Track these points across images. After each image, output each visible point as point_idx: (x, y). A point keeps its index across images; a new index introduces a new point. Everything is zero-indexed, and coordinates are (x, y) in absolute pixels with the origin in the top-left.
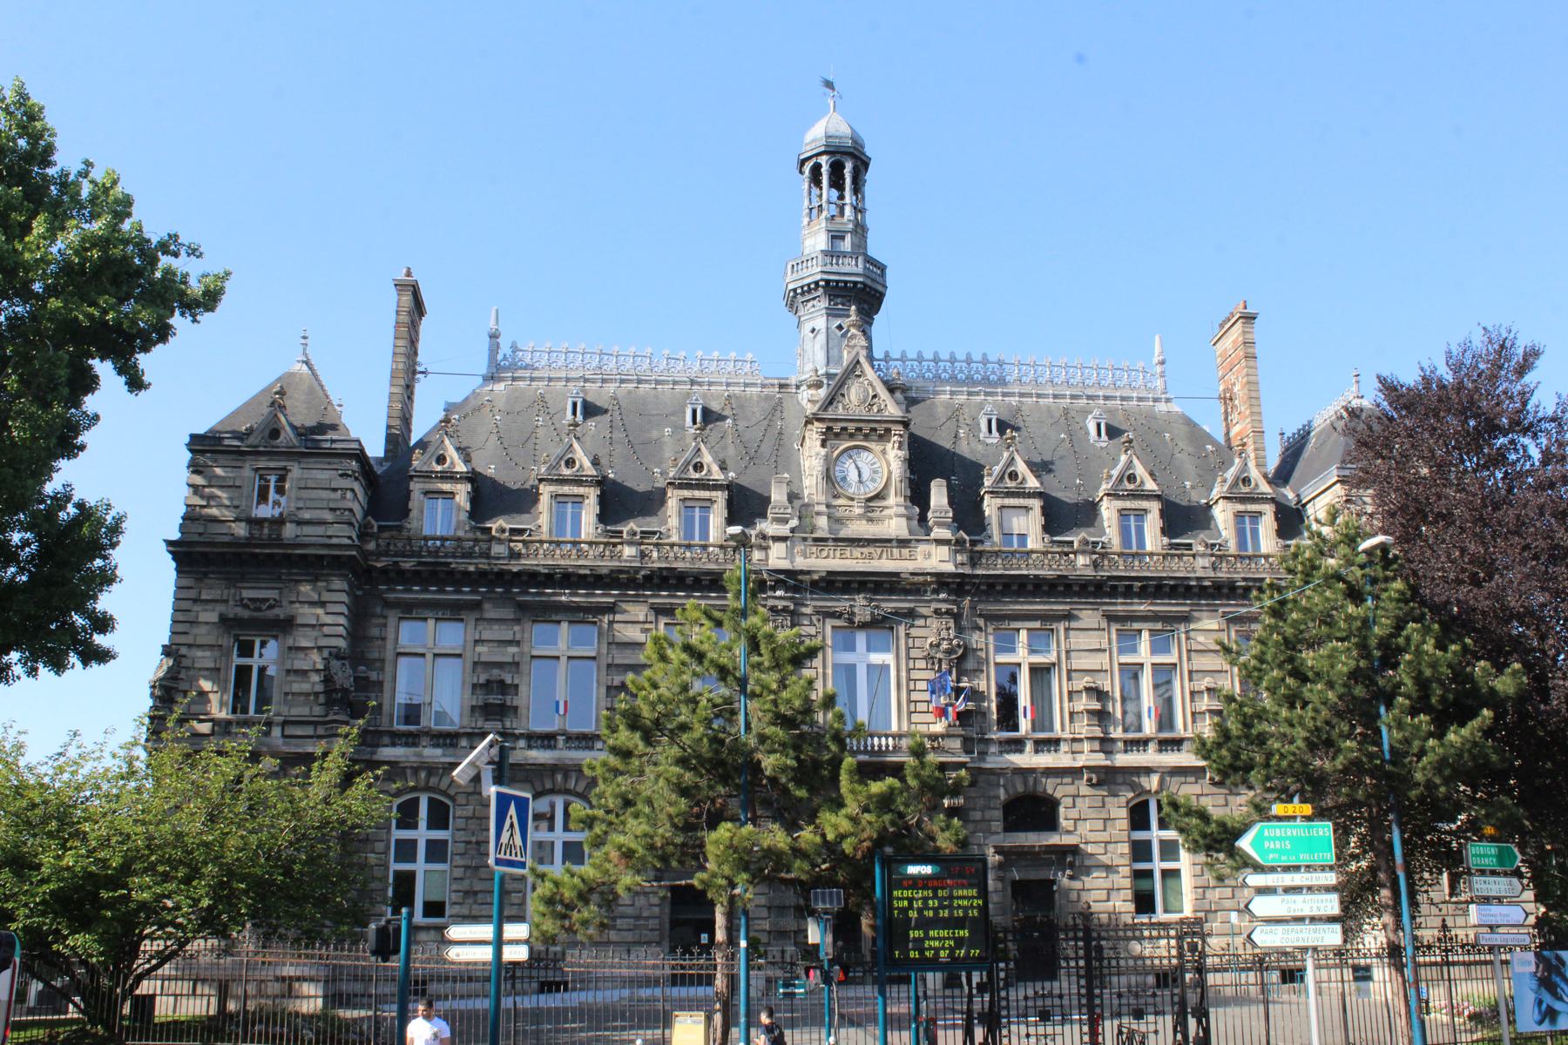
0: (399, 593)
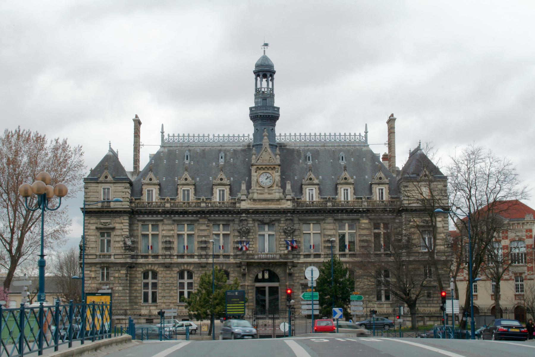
0: (141, 217)
